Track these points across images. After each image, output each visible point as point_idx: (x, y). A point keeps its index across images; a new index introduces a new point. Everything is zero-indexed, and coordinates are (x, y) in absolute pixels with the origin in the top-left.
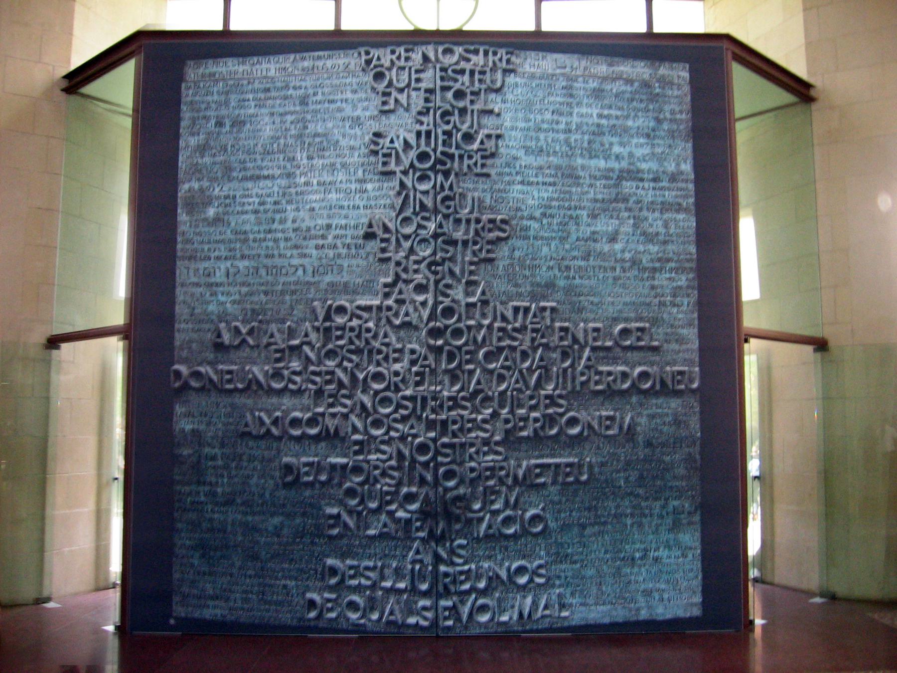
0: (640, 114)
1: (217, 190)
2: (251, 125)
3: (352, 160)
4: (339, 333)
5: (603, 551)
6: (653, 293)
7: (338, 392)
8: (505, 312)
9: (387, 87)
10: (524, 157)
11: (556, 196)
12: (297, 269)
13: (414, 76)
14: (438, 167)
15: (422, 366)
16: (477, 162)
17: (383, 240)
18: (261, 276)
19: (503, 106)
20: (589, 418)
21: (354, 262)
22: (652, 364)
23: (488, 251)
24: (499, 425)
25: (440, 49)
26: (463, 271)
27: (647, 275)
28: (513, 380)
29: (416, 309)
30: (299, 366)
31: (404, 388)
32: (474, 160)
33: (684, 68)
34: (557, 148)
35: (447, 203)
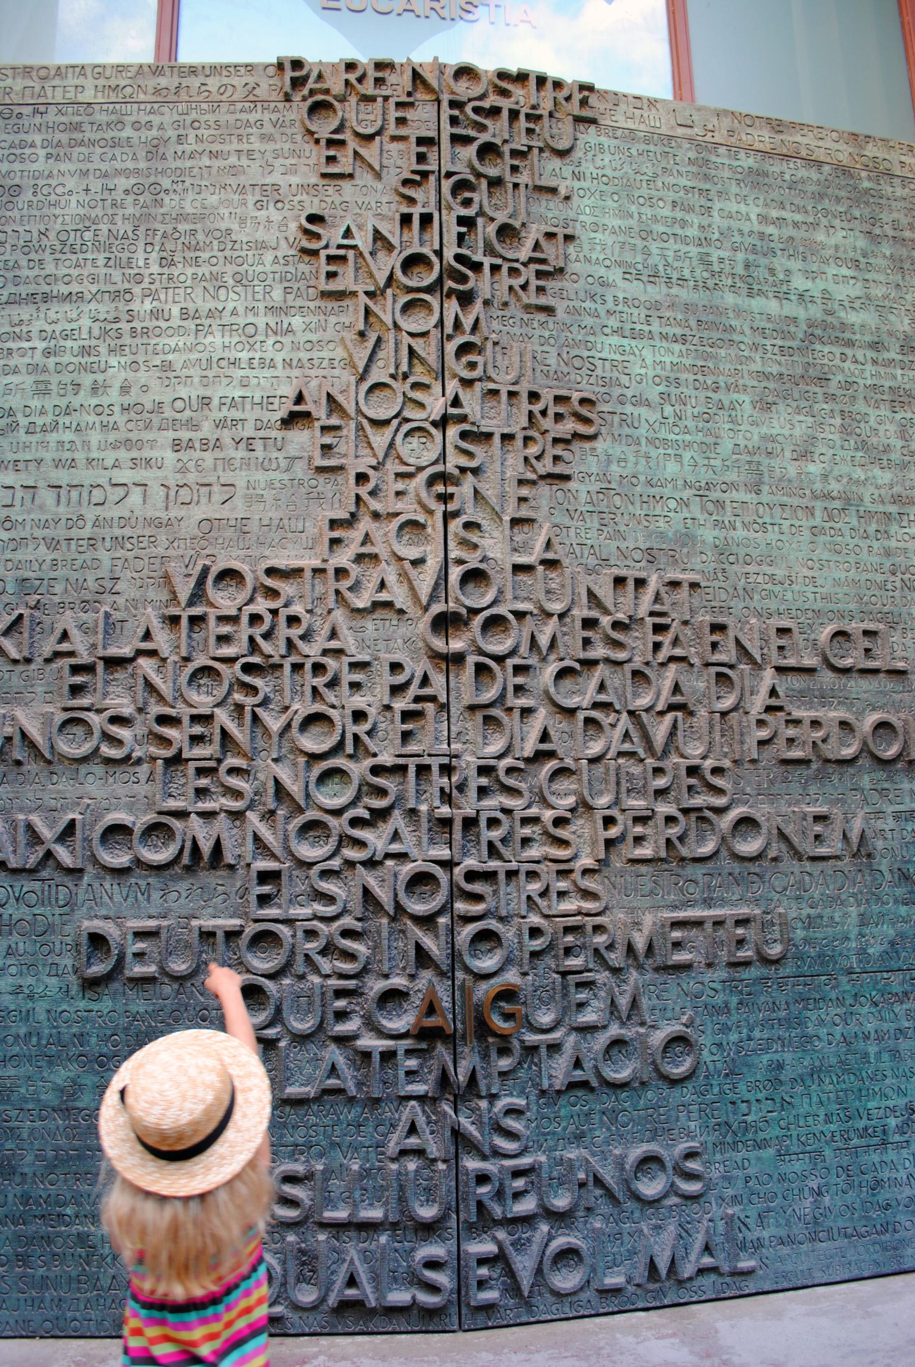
0: (837, 223)
3: (260, 269)
5: (822, 1117)
9: (335, 132)
10: (620, 283)
11: (688, 362)
16: (527, 282)
21: (260, 477)
22: (897, 708)
34: (686, 273)
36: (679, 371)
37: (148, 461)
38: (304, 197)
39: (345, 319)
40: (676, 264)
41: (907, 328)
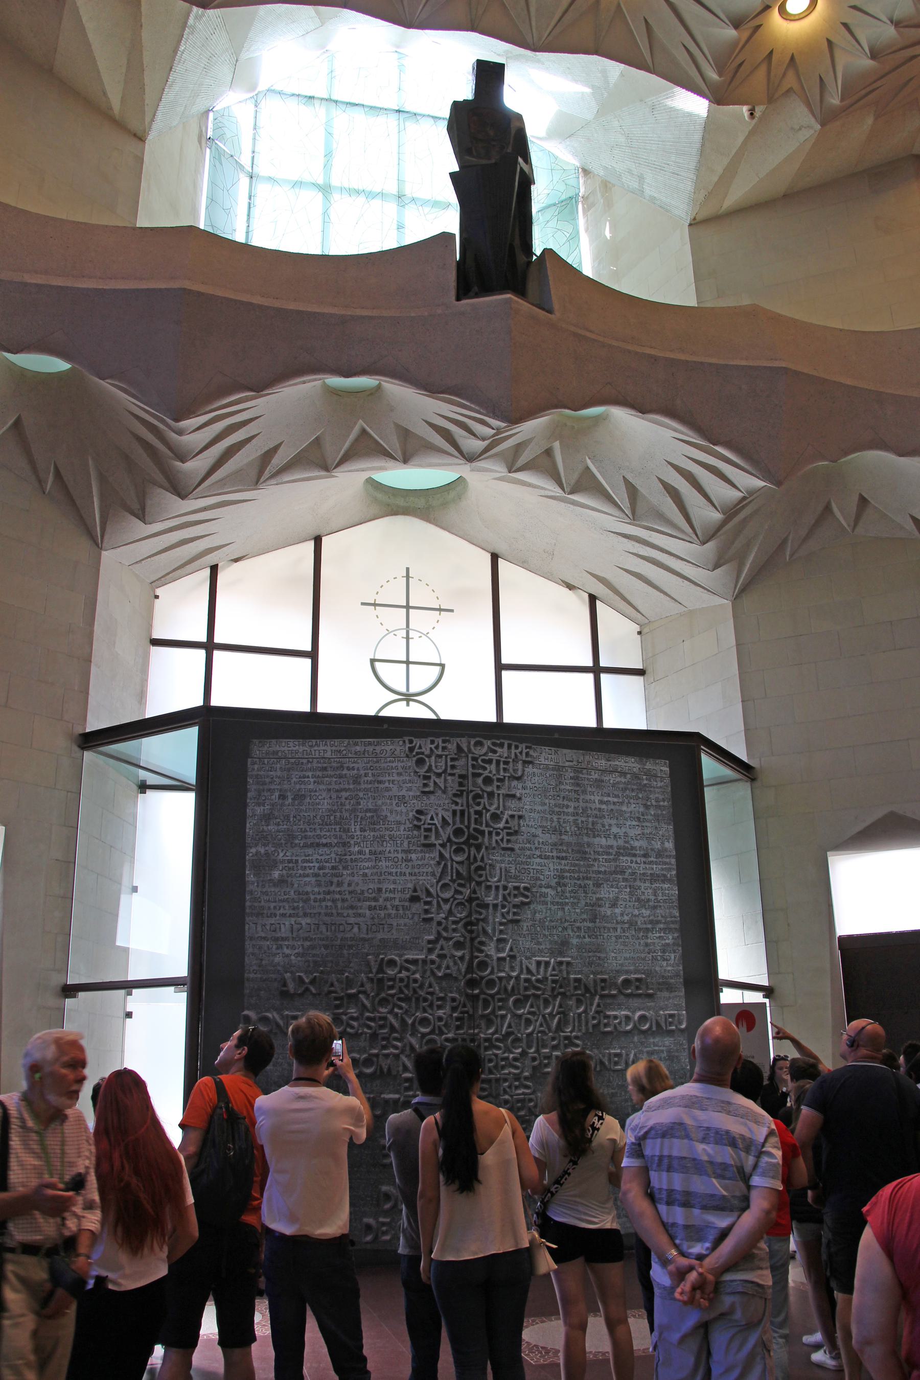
0: (632, 801)
1: (281, 854)
2: (310, 799)
3: (398, 833)
4: (391, 983)
6: (647, 950)
7: (390, 1035)
8: (530, 966)
10: (541, 835)
11: (567, 868)
12: (352, 928)
13: (449, 763)
14: (471, 841)
15: (461, 1013)
17: (426, 903)
18: (321, 932)
19: (524, 792)
20: (601, 1056)
21: (402, 921)
22: (649, 1009)
23: (514, 914)
24: (527, 1062)
25: (472, 743)
26: (494, 930)
27: (642, 934)
28: (538, 1024)
29: (455, 963)
30: (355, 1012)
31: (446, 1032)
32: (501, 837)
33: (665, 764)
34: (568, 828)
35: (480, 872)
36: (564, 872)
37: (360, 915)
38: (415, 801)
39: (432, 856)
40: (564, 825)
41: (659, 846)
